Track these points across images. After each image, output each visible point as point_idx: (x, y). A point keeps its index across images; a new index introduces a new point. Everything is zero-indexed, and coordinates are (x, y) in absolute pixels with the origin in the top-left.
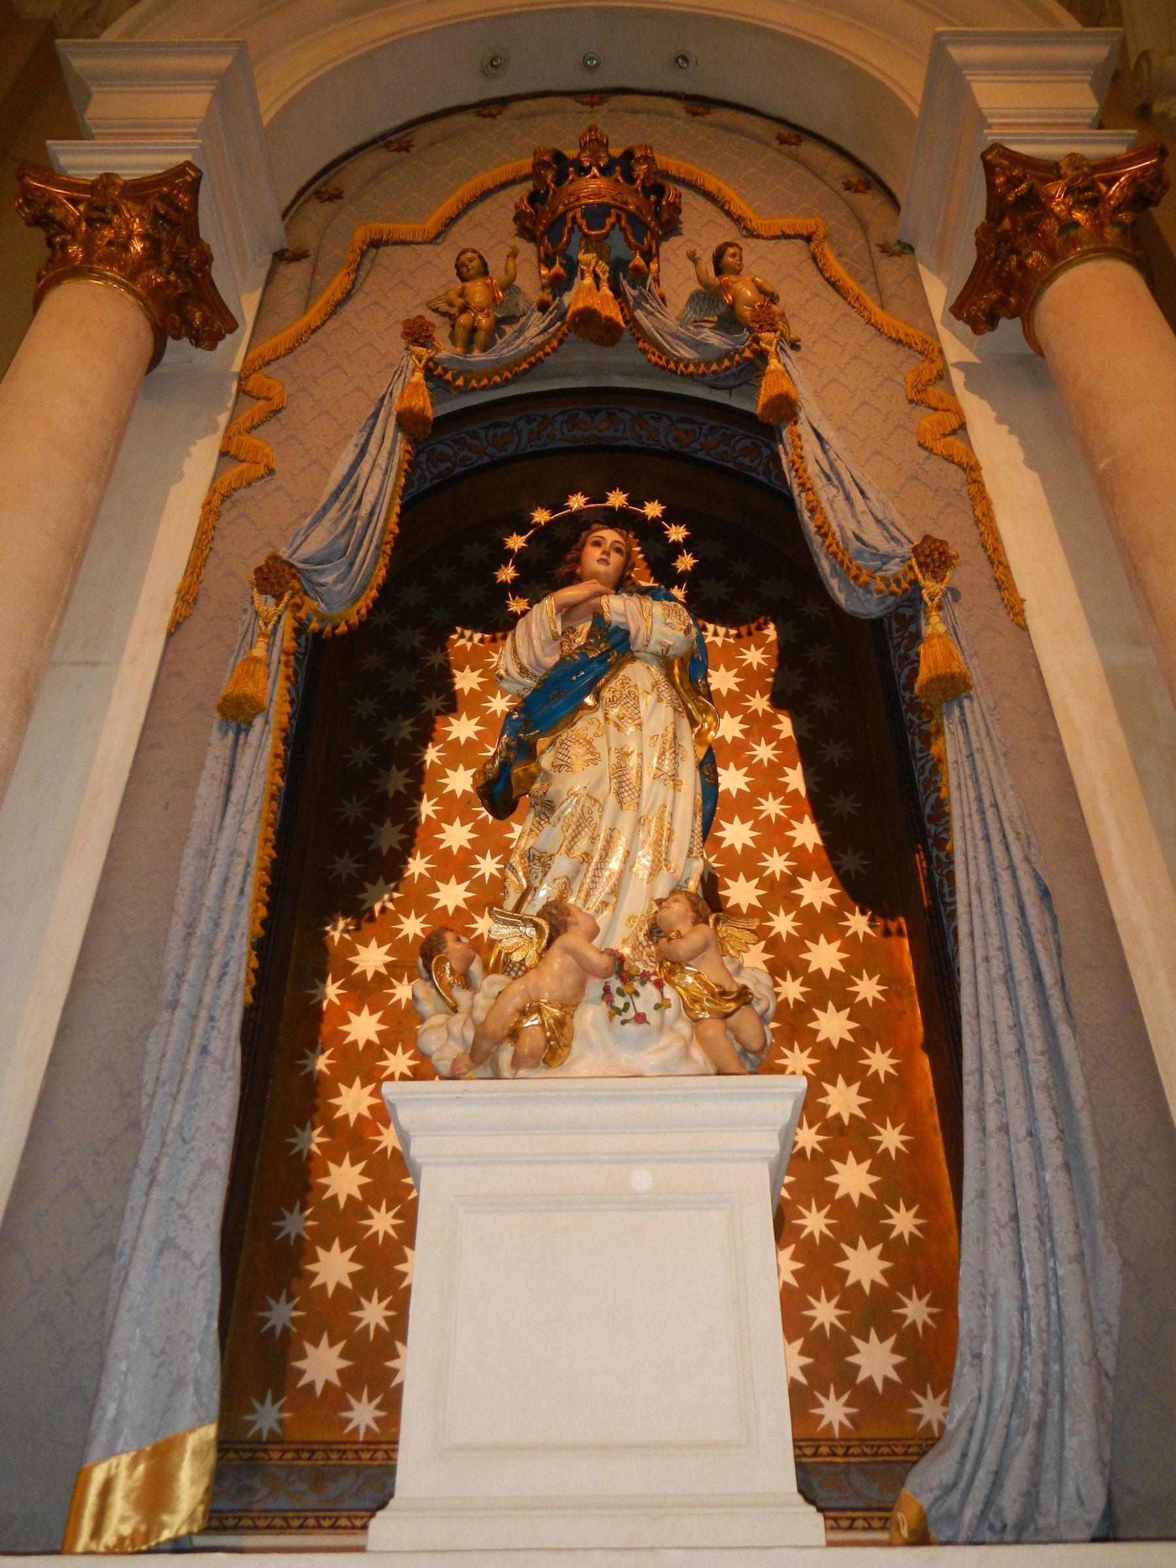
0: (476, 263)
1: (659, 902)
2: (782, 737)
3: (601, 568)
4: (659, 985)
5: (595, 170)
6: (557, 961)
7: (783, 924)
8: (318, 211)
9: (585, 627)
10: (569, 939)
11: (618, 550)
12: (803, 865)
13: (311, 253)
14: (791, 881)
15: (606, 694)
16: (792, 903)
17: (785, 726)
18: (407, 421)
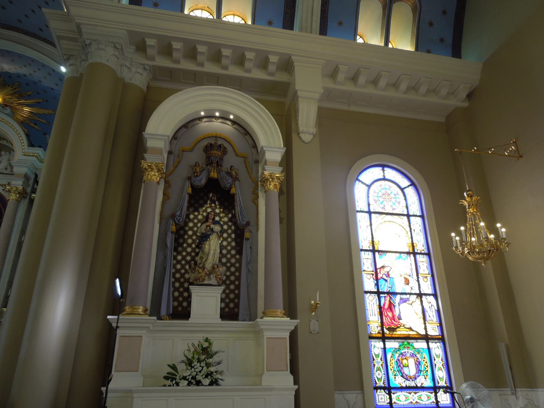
0: (198, 165)
1: (214, 264)
2: (232, 229)
3: (211, 218)
4: (213, 275)
5: (216, 150)
6: (204, 273)
7: (229, 256)
8: (175, 142)
9: (208, 228)
10: (206, 270)
11: (213, 215)
12: (233, 248)
13: (174, 152)
14: (230, 250)
15: (211, 239)
16: (230, 253)
17: (233, 228)
18: (189, 194)
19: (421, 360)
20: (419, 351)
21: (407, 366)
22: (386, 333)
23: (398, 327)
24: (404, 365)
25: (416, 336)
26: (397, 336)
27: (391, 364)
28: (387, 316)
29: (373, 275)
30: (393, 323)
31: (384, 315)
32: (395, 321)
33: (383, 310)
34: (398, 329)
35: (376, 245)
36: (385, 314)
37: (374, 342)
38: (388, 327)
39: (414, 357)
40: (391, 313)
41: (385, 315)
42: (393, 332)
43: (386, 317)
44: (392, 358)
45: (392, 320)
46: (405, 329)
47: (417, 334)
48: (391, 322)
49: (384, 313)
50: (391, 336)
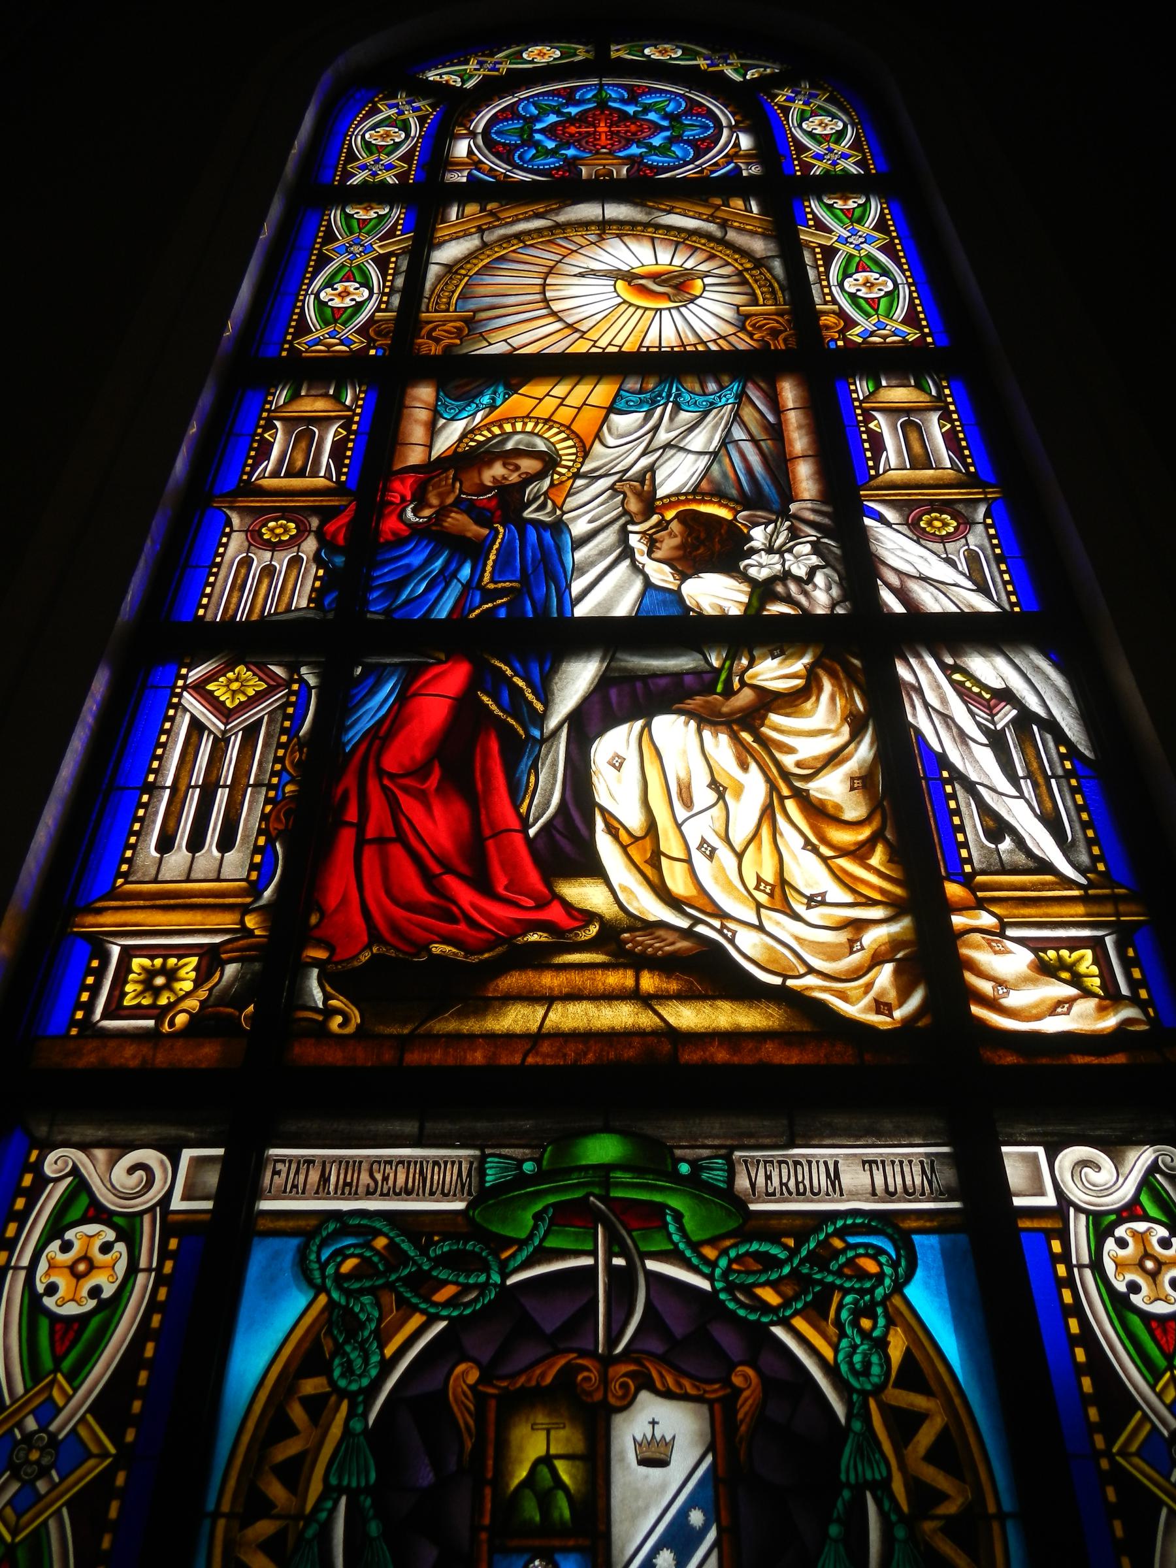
19: (859, 1411)
20: (822, 1257)
21: (564, 1509)
22: (321, 1031)
23: (538, 958)
24: (509, 1504)
25: (794, 1058)
26: (478, 1057)
27: (277, 1491)
28: (381, 841)
29: (327, 514)
30: (447, 911)
31: (347, 838)
32: (483, 884)
33: (349, 781)
34: (513, 981)
35: (437, 340)
36: (361, 827)
37: (84, 1147)
38: (365, 957)
39: (731, 1367)
40: (459, 808)
41: (370, 833)
42: (436, 1012)
43: (369, 853)
44: (311, 1386)
45: (448, 879)
46: (615, 979)
47: (806, 1027)
48: (426, 897)
49: (352, 815)
50: (388, 1056)
